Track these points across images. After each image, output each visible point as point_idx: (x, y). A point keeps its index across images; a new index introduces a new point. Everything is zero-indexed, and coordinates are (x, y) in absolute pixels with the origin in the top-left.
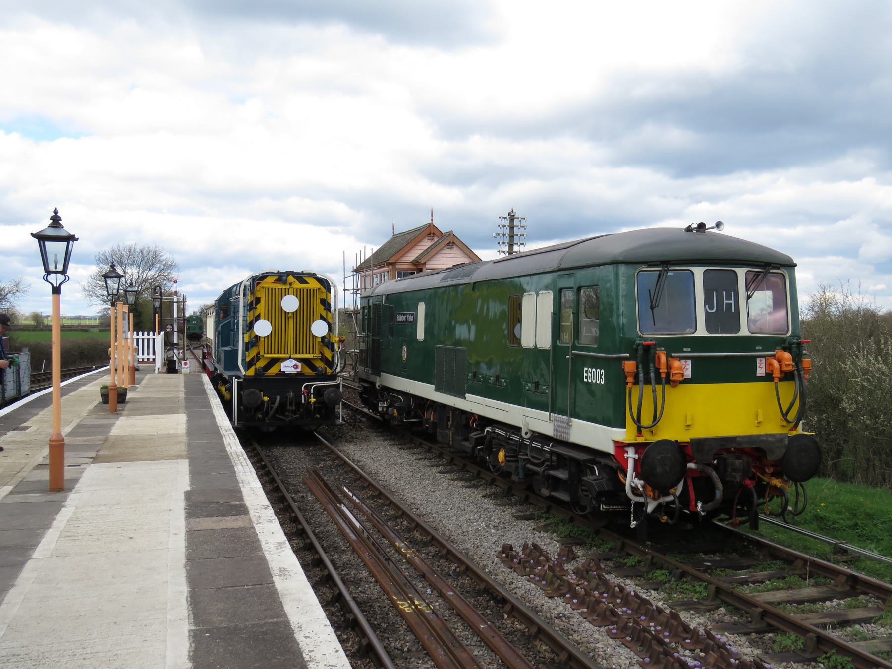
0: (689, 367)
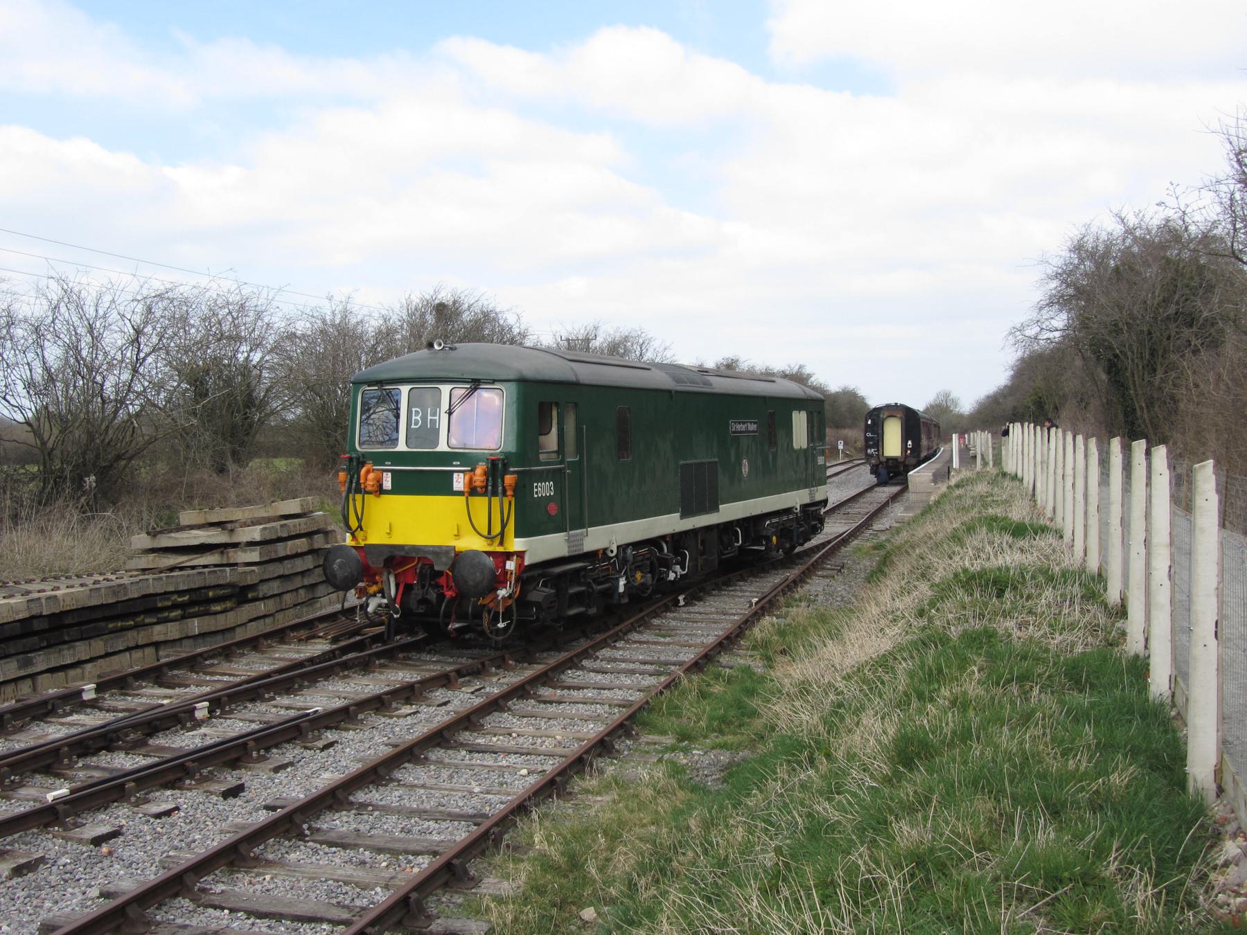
0: (390, 479)
